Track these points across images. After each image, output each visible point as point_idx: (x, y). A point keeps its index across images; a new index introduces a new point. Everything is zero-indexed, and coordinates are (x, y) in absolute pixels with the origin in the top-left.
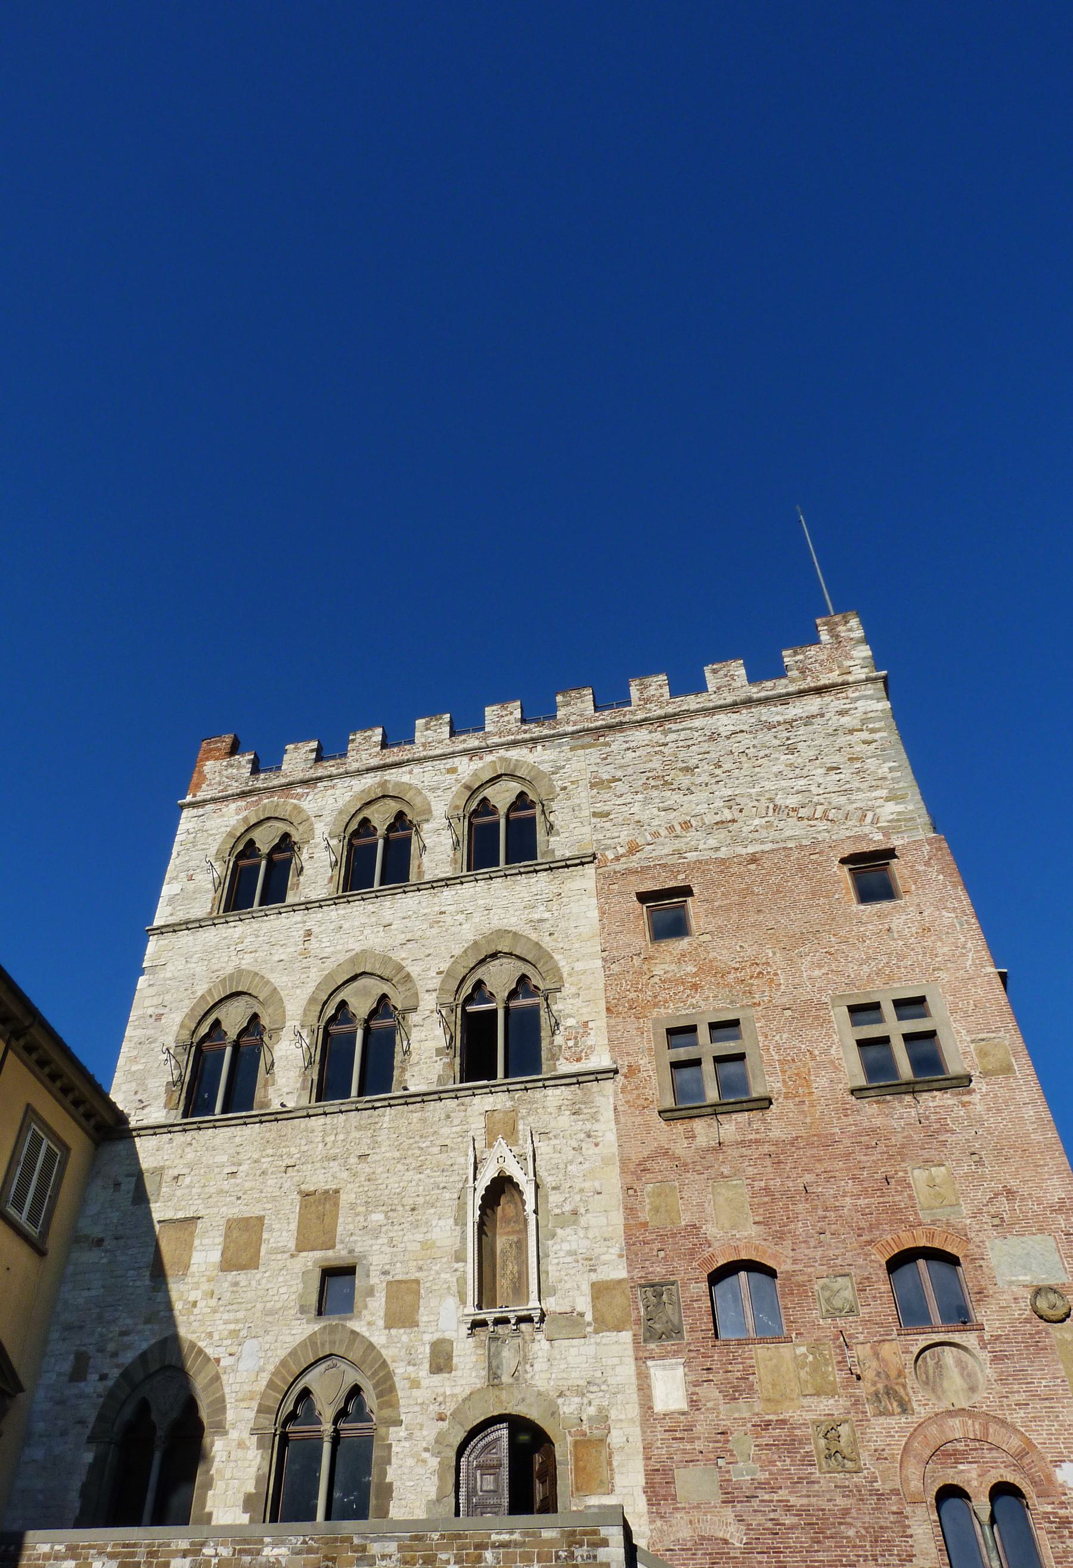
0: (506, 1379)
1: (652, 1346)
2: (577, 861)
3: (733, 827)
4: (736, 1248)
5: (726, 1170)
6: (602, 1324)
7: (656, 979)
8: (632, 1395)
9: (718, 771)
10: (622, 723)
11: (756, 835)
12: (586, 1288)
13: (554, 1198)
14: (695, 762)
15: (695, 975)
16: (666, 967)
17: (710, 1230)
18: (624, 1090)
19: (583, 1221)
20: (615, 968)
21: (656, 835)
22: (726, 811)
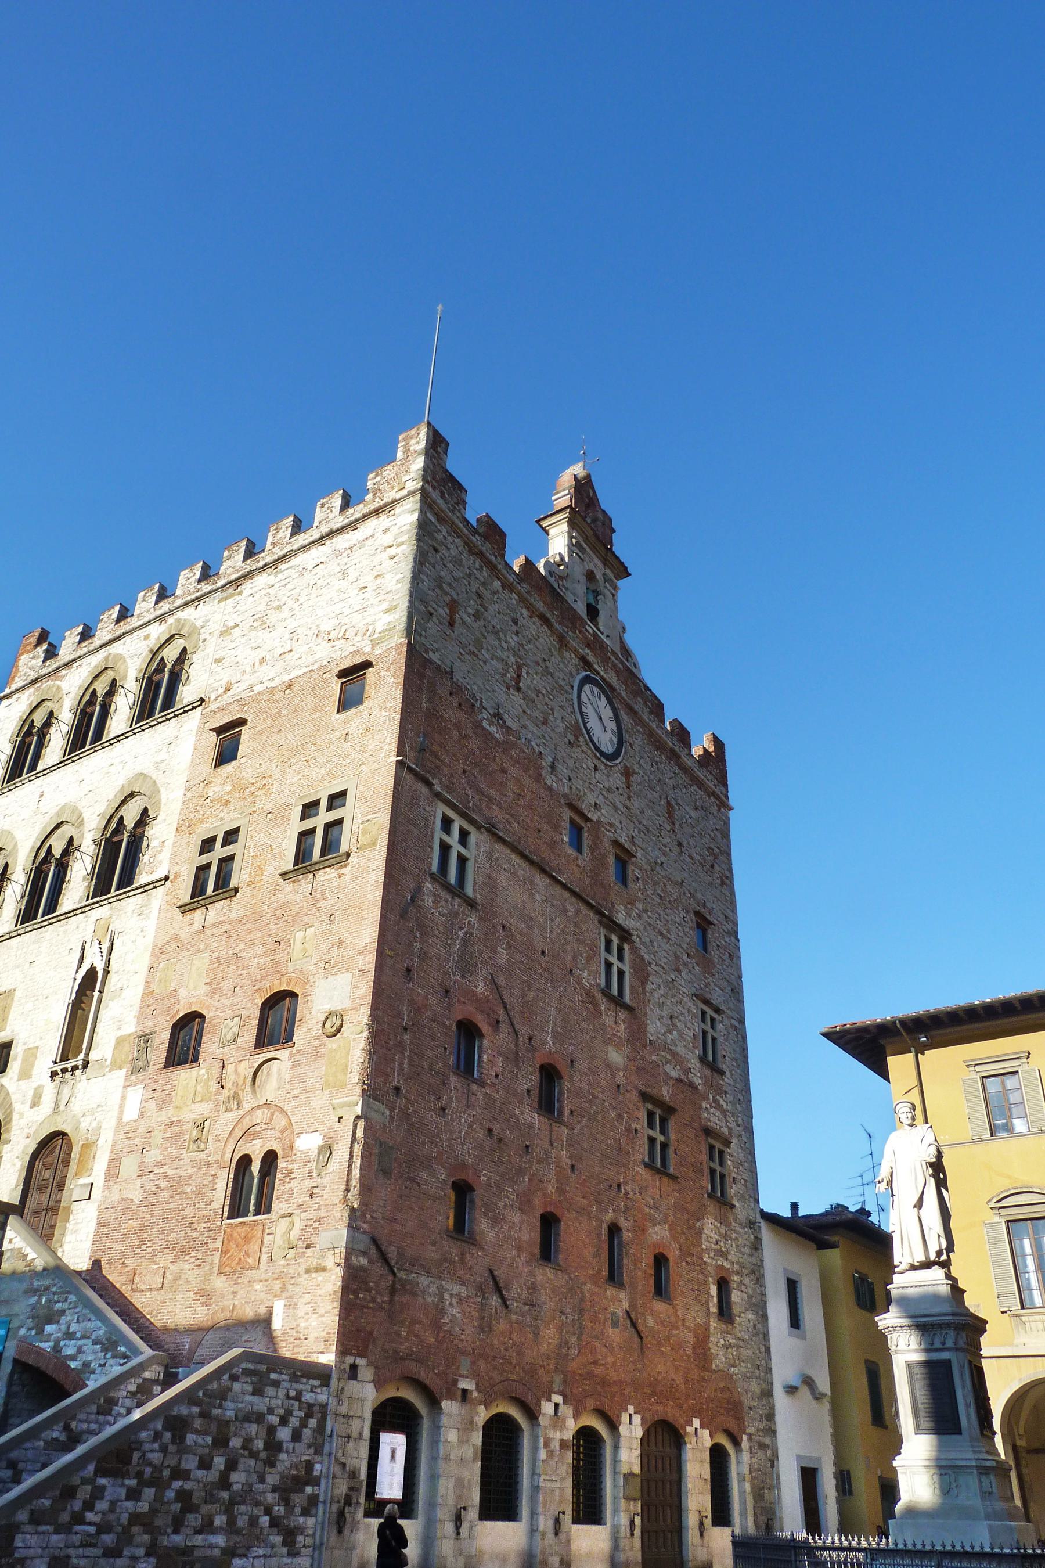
0: (62, 1108)
1: (133, 1077)
2: (190, 707)
3: (288, 656)
4: (191, 1004)
5: (202, 947)
6: (115, 1065)
7: (208, 801)
8: (115, 1113)
9: (295, 606)
10: (251, 572)
11: (299, 662)
12: (113, 1043)
13: (112, 978)
14: (285, 599)
15: (229, 793)
16: (216, 789)
17: (182, 993)
18: (168, 893)
19: (125, 993)
20: (189, 795)
21: (243, 673)
22: (289, 642)
